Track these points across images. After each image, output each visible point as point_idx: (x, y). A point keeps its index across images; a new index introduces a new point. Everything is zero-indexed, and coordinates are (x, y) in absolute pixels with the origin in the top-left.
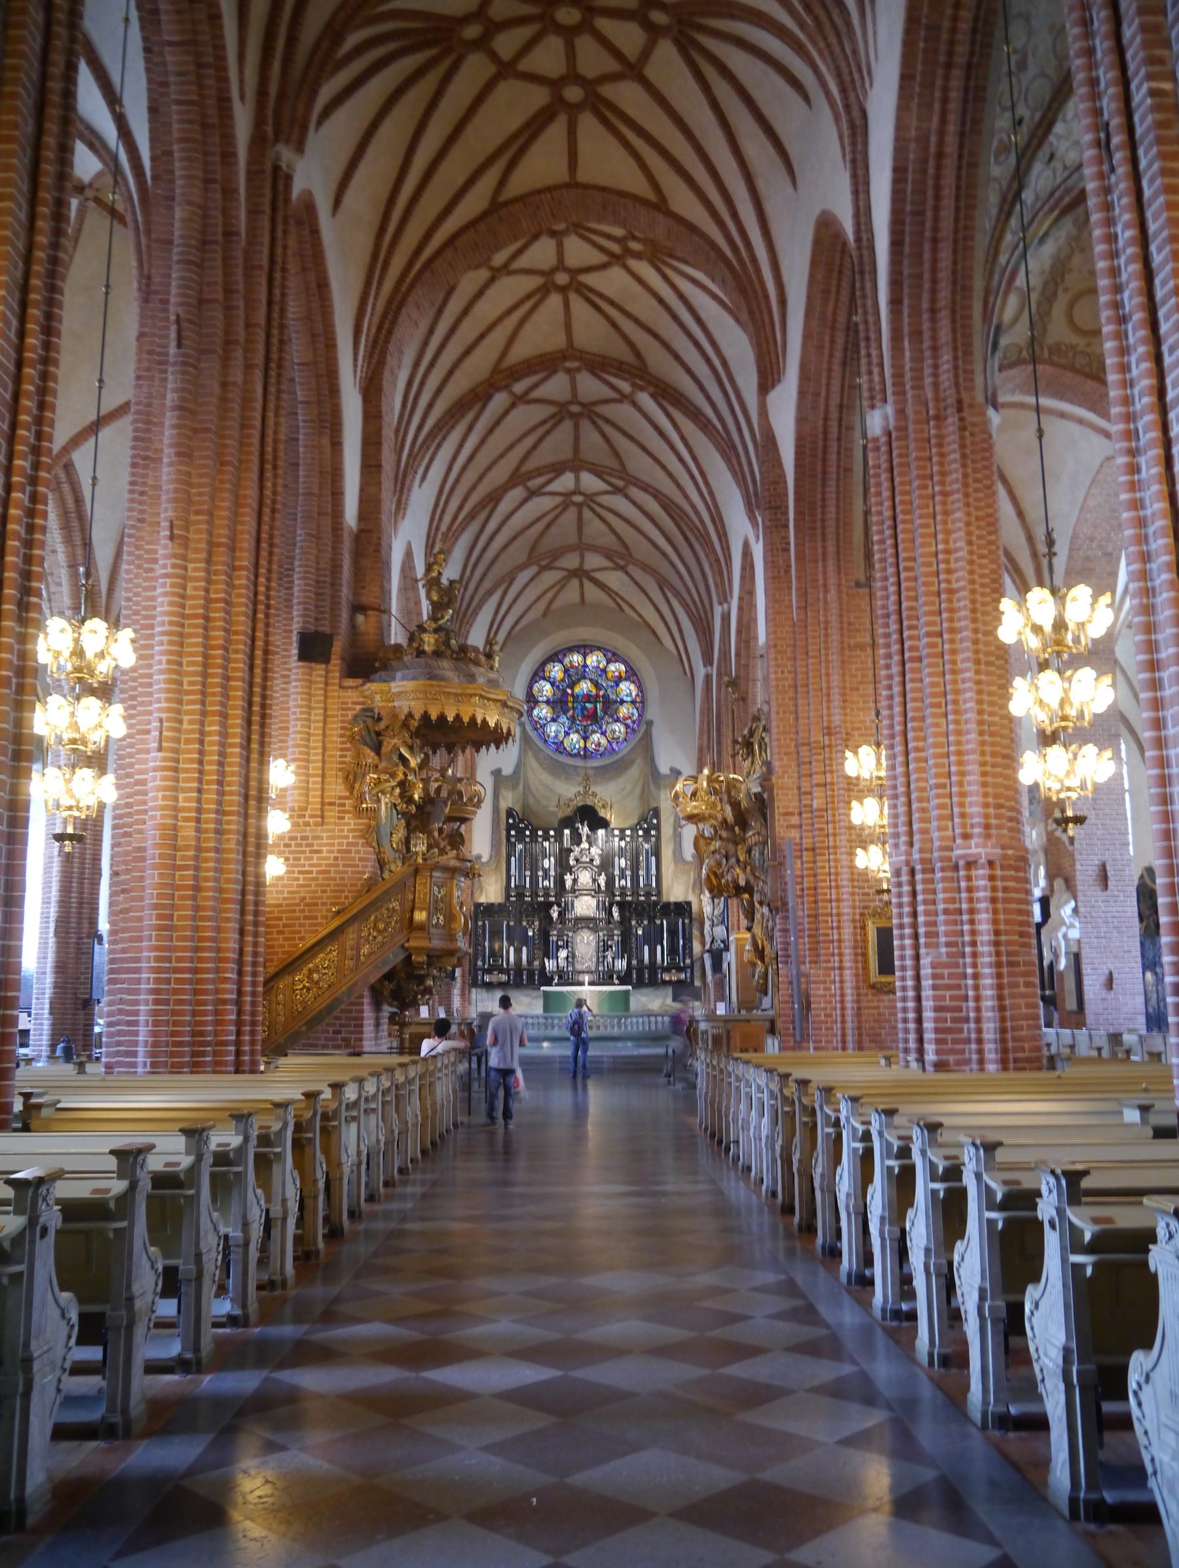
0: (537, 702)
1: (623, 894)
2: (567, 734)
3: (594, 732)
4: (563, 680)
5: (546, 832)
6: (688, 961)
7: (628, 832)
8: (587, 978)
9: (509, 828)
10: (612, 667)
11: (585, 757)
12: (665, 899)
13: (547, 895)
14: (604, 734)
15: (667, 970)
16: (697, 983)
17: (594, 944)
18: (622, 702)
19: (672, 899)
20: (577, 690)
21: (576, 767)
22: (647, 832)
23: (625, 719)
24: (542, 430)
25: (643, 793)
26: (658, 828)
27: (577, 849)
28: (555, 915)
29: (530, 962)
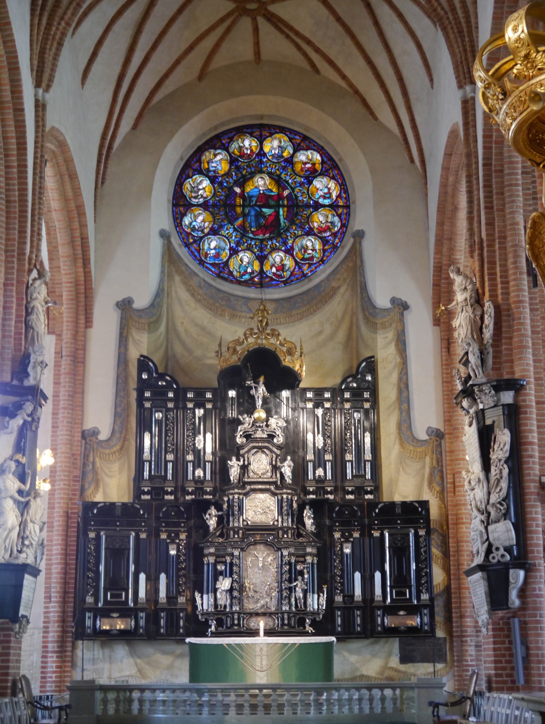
0: (189, 206)
1: (321, 490)
2: (234, 252)
3: (274, 249)
4: (228, 174)
5: (200, 393)
6: (425, 597)
7: (327, 395)
8: (262, 624)
9: (142, 386)
10: (302, 156)
11: (261, 285)
12: (386, 498)
13: (199, 490)
14: (289, 251)
15: (391, 610)
16: (440, 633)
17: (273, 569)
18: (317, 206)
19: (398, 498)
20: (249, 188)
21: (249, 299)
22: (357, 394)
23: (322, 230)
24: (220, 30)
25: (349, 337)
26: (374, 389)
27: (247, 420)
28: (212, 523)
29: (171, 598)
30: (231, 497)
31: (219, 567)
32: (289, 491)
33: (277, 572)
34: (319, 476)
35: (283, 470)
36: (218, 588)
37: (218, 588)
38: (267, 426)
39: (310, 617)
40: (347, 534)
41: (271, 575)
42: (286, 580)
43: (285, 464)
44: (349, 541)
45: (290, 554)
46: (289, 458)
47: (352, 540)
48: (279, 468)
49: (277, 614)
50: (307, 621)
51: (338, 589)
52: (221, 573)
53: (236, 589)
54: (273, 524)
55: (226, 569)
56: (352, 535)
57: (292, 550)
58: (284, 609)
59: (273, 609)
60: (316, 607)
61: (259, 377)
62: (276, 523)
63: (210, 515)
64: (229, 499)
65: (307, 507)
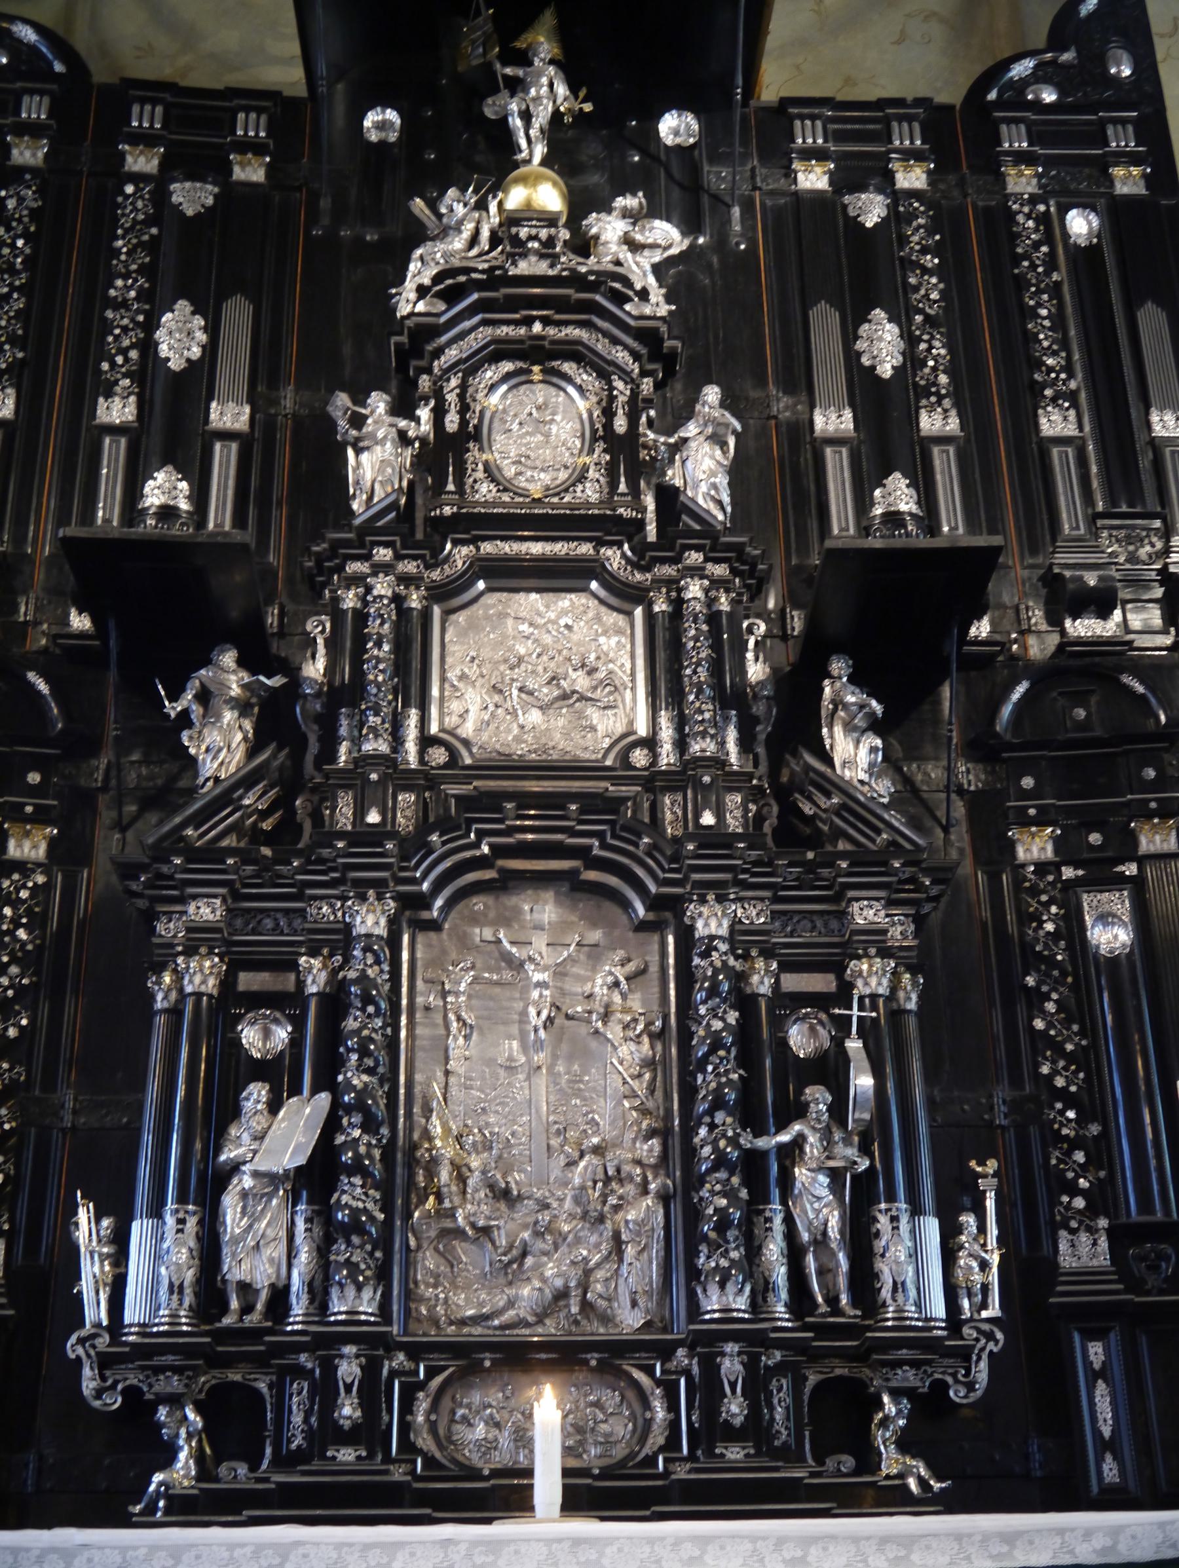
30: (350, 600)
31: (250, 1036)
32: (720, 570)
33: (649, 1063)
34: (894, 519)
35: (673, 476)
36: (235, 1168)
37: (235, 1168)
38: (584, 245)
39: (908, 1377)
40: (1095, 838)
41: (615, 1082)
42: (718, 1103)
43: (691, 429)
44: (1121, 881)
45: (738, 934)
46: (712, 394)
47: (1131, 869)
48: (655, 468)
49: (665, 1351)
50: (889, 1405)
51: (1074, 1191)
52: (263, 1070)
53: (358, 1168)
54: (624, 756)
55: (296, 1042)
56: (1132, 839)
57: (755, 915)
58: (712, 1302)
59: (630, 1320)
60: (938, 1309)
61: (527, 22)
62: (639, 758)
63: (204, 697)
64: (337, 615)
65: (839, 666)
